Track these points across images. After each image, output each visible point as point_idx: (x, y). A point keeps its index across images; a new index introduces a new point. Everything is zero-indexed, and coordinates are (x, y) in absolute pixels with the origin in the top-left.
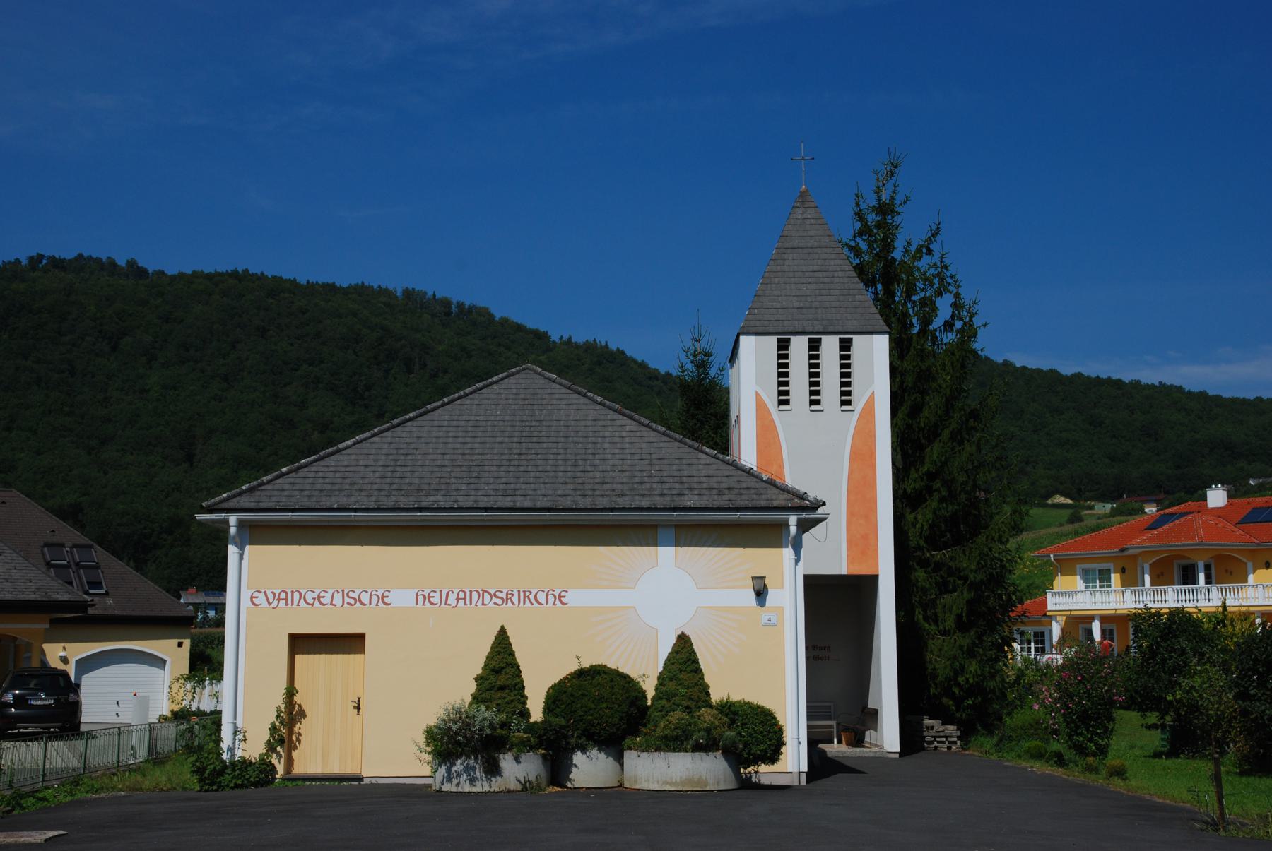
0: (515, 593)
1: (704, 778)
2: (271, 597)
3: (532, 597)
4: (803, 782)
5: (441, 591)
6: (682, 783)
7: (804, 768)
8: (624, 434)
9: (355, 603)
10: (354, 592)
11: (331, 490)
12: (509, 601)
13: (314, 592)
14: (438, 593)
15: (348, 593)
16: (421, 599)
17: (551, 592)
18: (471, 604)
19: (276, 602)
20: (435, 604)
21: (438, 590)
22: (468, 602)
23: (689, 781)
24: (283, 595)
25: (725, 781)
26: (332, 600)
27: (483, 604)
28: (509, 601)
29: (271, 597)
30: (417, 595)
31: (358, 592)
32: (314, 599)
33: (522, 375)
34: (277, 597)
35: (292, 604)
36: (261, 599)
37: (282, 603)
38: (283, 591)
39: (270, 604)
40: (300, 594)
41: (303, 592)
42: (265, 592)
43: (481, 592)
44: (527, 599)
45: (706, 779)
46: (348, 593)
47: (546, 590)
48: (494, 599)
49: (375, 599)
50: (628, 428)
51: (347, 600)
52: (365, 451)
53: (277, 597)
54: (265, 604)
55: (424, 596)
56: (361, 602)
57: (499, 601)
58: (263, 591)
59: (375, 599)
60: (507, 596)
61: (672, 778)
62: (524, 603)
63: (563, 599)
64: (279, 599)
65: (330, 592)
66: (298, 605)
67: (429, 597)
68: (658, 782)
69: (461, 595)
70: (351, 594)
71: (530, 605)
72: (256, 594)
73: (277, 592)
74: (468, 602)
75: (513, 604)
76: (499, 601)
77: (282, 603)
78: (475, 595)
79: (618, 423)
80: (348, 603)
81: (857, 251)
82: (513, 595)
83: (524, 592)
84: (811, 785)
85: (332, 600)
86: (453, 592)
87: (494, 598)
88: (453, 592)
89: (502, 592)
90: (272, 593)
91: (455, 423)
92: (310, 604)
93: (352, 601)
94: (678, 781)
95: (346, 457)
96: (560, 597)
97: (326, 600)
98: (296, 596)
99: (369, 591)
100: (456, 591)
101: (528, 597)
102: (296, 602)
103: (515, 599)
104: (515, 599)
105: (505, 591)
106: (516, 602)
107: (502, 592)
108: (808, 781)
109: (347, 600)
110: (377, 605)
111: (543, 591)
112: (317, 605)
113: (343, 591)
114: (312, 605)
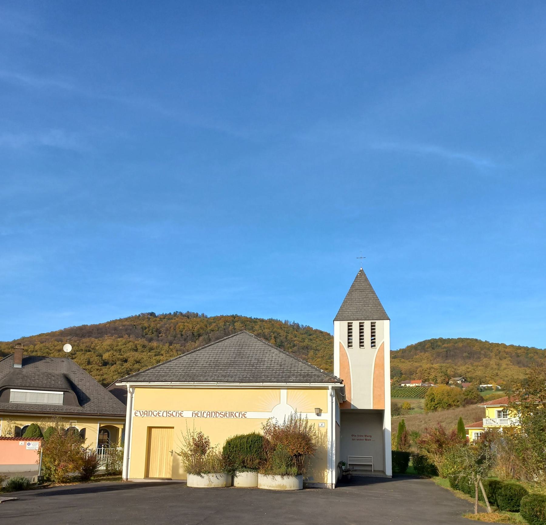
0: (228, 413)
1: (285, 485)
2: (142, 413)
3: (234, 414)
4: (334, 488)
5: (201, 412)
6: (276, 487)
7: (334, 482)
8: (274, 355)
9: (171, 416)
10: (170, 412)
11: (164, 375)
12: (225, 416)
13: (156, 411)
14: (200, 412)
15: (168, 412)
16: (194, 415)
17: (194, 412)
18: (212, 417)
19: (143, 415)
20: (160, 416)
21: (200, 412)
22: (148, 415)
23: (279, 486)
24: (146, 413)
25: (294, 487)
26: (163, 415)
27: (216, 417)
28: (225, 416)
29: (142, 413)
30: (193, 413)
31: (172, 412)
32: (157, 414)
33: (242, 334)
34: (144, 413)
35: (149, 416)
36: (138, 414)
37: (146, 415)
38: (146, 411)
39: (141, 416)
40: (152, 412)
41: (153, 411)
42: (140, 411)
43: (215, 413)
44: (232, 415)
45: (286, 486)
46: (168, 412)
47: (239, 412)
48: (220, 415)
49: (178, 414)
50: (275, 353)
51: (168, 414)
52: (180, 361)
53: (144, 413)
54: (140, 415)
55: (242, 414)
56: (173, 416)
57: (222, 416)
58: (139, 411)
59: (178, 414)
60: (225, 414)
61: (272, 485)
62: (231, 417)
63: (245, 416)
64: (144, 414)
65: (162, 411)
66: (151, 416)
67: (197, 414)
68: (268, 486)
69: (208, 413)
70: (169, 413)
71: (226, 417)
72: (136, 412)
73: (144, 411)
74: (148, 415)
75: (227, 417)
76: (222, 416)
77: (146, 415)
78: (213, 414)
79: (272, 351)
80: (168, 416)
81: (126, 330)
82: (227, 414)
83: (231, 413)
84: (336, 489)
85: (163, 415)
86: (205, 412)
87: (220, 415)
88: (205, 412)
89: (223, 412)
90: (142, 411)
91: (214, 351)
92: (155, 416)
93: (170, 415)
94: (275, 486)
95: (172, 363)
96: (181, 414)
97: (161, 415)
98: (150, 413)
99: (176, 411)
100: (207, 412)
101: (232, 414)
102: (150, 415)
103: (228, 415)
104: (228, 415)
105: (224, 412)
106: (228, 416)
107: (223, 412)
108: (335, 487)
109: (168, 414)
110: (178, 416)
111: (238, 413)
112: (157, 416)
113: (167, 411)
114: (156, 416)
